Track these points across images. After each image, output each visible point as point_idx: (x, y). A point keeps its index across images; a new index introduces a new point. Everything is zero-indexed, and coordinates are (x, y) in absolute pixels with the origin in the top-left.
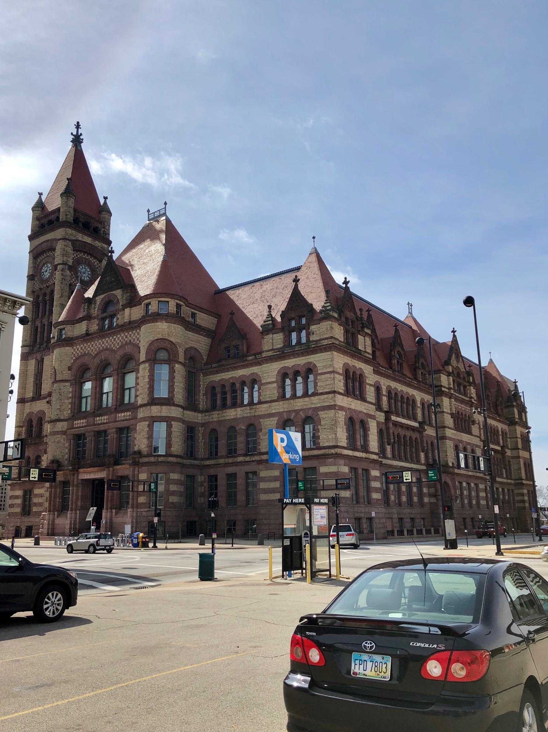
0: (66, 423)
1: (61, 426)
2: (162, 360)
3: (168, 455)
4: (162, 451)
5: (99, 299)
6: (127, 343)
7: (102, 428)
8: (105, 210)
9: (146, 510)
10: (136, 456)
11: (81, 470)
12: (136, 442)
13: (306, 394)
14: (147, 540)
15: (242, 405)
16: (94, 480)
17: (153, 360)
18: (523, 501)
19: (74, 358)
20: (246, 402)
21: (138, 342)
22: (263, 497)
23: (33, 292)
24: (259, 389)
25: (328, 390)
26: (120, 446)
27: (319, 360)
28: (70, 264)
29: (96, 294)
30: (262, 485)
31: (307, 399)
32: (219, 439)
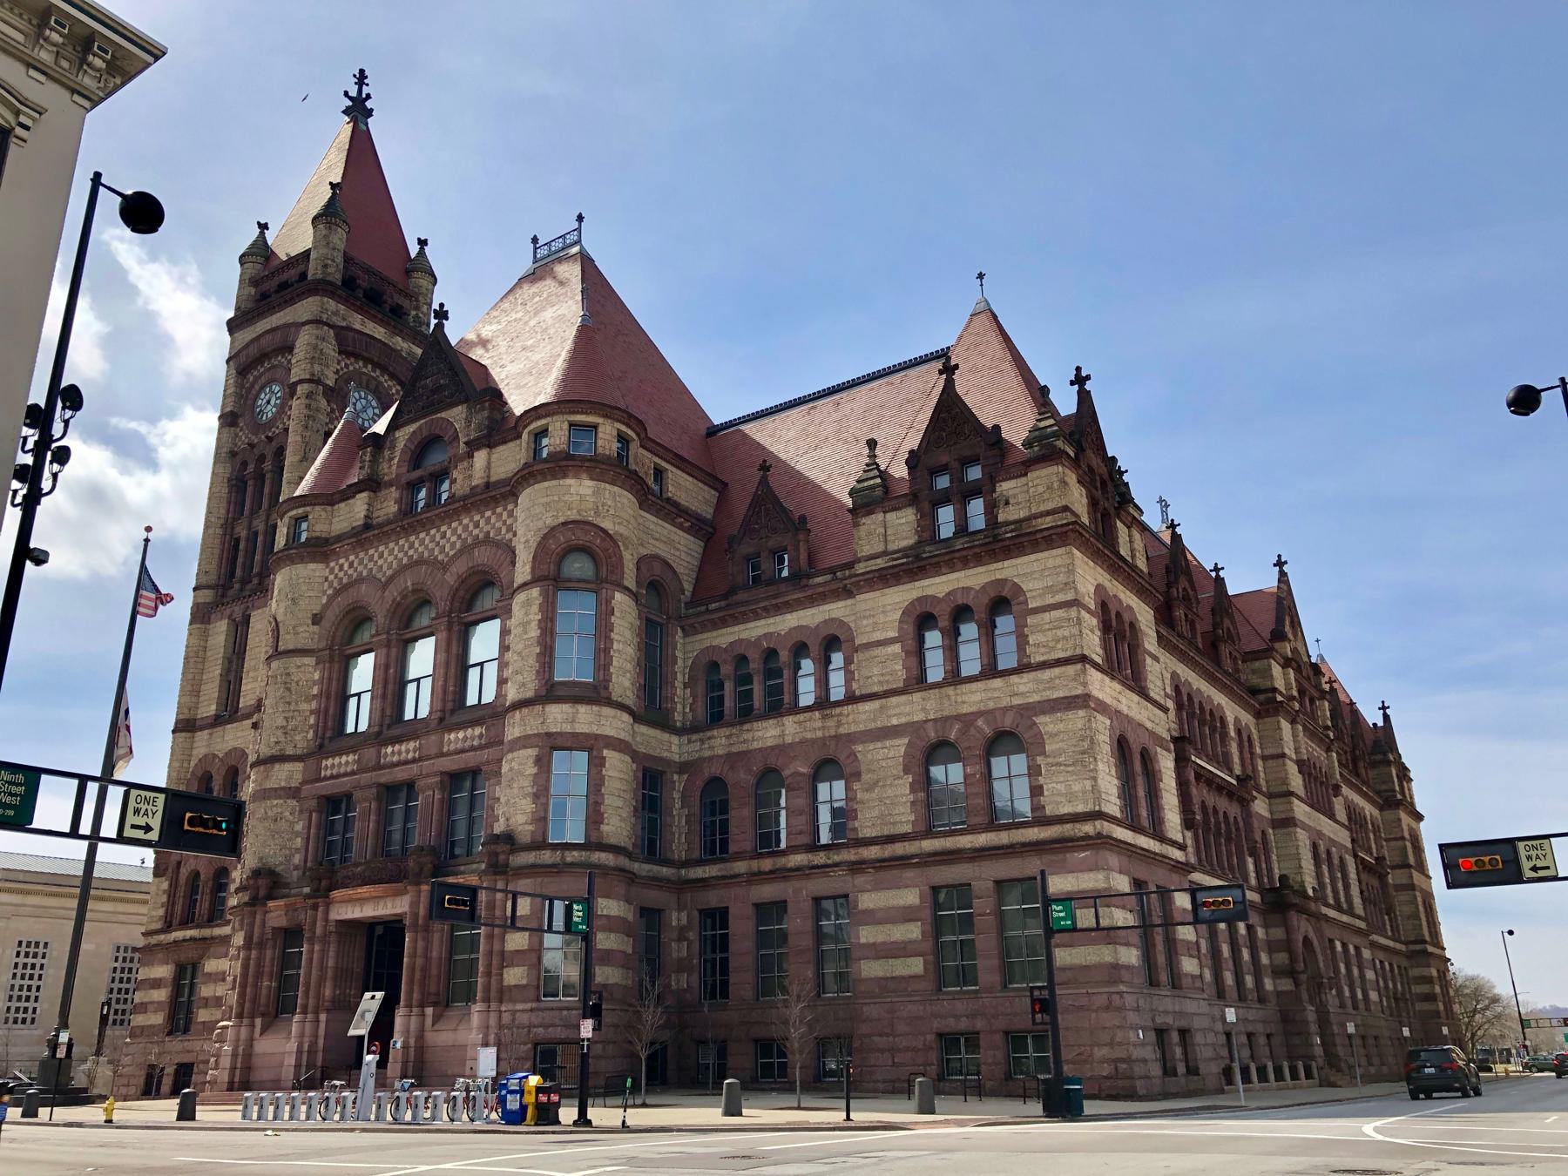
0: (298, 767)
1: (285, 774)
2: (579, 581)
3: (593, 844)
4: (574, 832)
5: (403, 435)
6: (478, 543)
7: (400, 774)
8: (419, 269)
9: (529, 1006)
10: (499, 848)
11: (336, 894)
12: (499, 810)
13: (991, 670)
14: (555, 1098)
15: (795, 709)
16: (369, 926)
17: (551, 579)
18: (1431, 998)
19: (330, 592)
20: (806, 699)
21: (509, 536)
22: (871, 969)
23: (233, 454)
24: (848, 661)
25: (1061, 655)
26: (449, 828)
27: (1031, 573)
28: (331, 383)
29: (393, 426)
30: (867, 935)
31: (997, 683)
32: (732, 804)
